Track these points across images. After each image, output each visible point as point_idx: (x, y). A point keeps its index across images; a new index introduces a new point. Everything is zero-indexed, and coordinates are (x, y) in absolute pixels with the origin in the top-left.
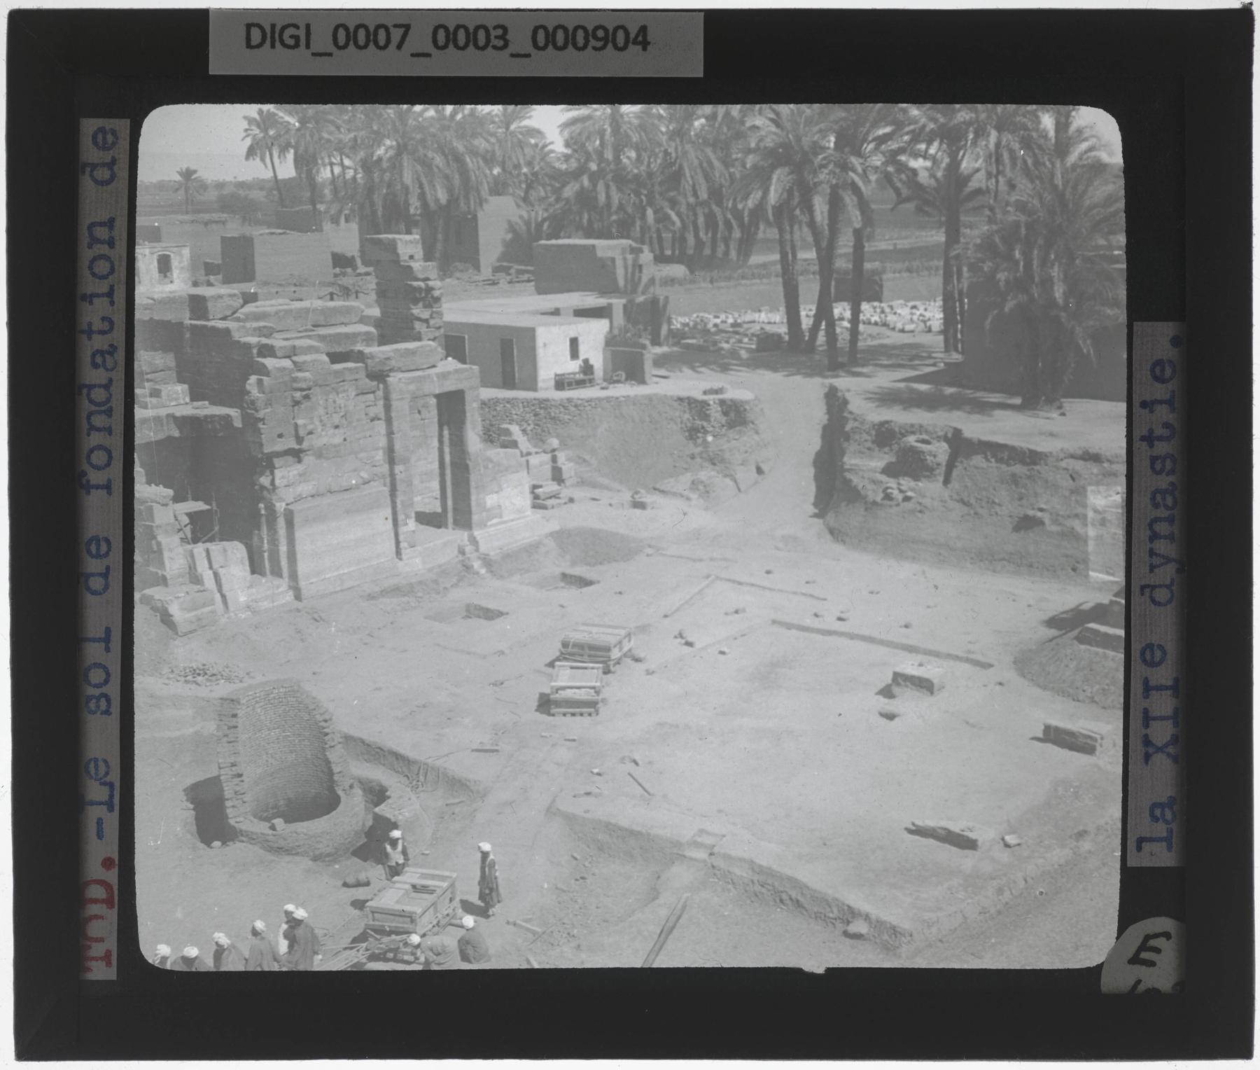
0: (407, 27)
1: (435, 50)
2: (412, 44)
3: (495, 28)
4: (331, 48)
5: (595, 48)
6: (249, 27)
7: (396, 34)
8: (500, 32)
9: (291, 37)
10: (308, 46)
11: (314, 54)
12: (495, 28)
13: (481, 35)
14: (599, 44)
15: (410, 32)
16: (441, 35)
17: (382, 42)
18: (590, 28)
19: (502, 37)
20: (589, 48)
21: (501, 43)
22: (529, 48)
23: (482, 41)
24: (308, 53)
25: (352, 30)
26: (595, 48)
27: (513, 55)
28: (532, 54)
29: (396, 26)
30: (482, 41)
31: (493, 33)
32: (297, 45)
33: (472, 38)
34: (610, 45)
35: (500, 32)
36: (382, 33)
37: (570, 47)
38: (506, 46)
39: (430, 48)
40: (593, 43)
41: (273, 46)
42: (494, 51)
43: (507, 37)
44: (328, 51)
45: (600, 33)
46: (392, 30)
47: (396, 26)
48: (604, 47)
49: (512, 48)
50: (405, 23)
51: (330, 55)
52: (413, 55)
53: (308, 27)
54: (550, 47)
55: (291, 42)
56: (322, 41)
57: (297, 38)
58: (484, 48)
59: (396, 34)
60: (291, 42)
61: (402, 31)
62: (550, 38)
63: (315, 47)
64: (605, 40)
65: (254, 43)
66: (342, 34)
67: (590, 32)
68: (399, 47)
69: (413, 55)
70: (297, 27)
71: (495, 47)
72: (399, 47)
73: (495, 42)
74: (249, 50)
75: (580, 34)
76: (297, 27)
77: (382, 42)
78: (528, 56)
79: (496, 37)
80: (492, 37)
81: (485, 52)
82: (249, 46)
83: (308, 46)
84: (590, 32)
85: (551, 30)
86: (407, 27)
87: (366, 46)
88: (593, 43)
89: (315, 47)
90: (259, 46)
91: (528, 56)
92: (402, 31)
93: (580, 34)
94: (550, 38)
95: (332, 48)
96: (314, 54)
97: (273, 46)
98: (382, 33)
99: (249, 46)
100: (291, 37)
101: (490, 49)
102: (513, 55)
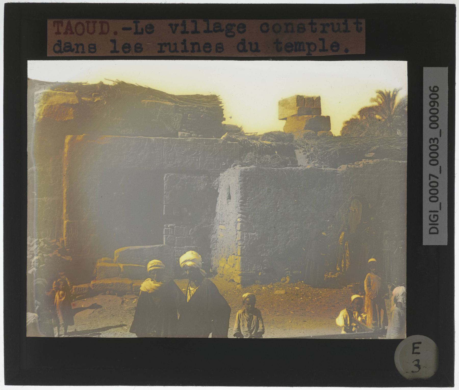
2: (437, 173)
3: (430, 143)
4: (438, 203)
5: (438, 106)
6: (430, 233)
7: (433, 179)
8: (432, 141)
9: (434, 218)
10: (437, 212)
11: (440, 209)
12: (430, 143)
13: (433, 148)
15: (432, 174)
16: (432, 162)
18: (431, 108)
20: (437, 108)
21: (436, 141)
22: (438, 130)
23: (435, 148)
26: (438, 106)
29: (430, 179)
30: (435, 148)
31: (432, 143)
32: (437, 216)
33: (434, 151)
34: (436, 100)
35: (432, 141)
36: (432, 184)
40: (436, 107)
41: (437, 224)
42: (439, 143)
43: (434, 138)
44: (439, 203)
45: (432, 104)
46: (431, 180)
47: (430, 179)
50: (429, 175)
52: (440, 173)
53: (430, 211)
55: (436, 217)
56: (435, 206)
57: (434, 216)
59: (433, 179)
61: (431, 176)
62: (434, 122)
63: (438, 209)
64: (434, 91)
65: (437, 232)
66: (432, 199)
68: (437, 178)
69: (440, 173)
70: (430, 215)
71: (437, 143)
72: (437, 178)
73: (435, 143)
74: (439, 233)
75: (433, 111)
77: (435, 184)
79: (434, 142)
80: (434, 144)
81: (439, 146)
83: (437, 212)
85: (431, 122)
87: (437, 190)
88: (436, 107)
89: (438, 209)
90: (437, 229)
93: (432, 111)
94: (434, 122)
95: (438, 202)
96: (440, 209)
97: (437, 224)
98: (432, 184)
100: (434, 218)
101: (437, 144)
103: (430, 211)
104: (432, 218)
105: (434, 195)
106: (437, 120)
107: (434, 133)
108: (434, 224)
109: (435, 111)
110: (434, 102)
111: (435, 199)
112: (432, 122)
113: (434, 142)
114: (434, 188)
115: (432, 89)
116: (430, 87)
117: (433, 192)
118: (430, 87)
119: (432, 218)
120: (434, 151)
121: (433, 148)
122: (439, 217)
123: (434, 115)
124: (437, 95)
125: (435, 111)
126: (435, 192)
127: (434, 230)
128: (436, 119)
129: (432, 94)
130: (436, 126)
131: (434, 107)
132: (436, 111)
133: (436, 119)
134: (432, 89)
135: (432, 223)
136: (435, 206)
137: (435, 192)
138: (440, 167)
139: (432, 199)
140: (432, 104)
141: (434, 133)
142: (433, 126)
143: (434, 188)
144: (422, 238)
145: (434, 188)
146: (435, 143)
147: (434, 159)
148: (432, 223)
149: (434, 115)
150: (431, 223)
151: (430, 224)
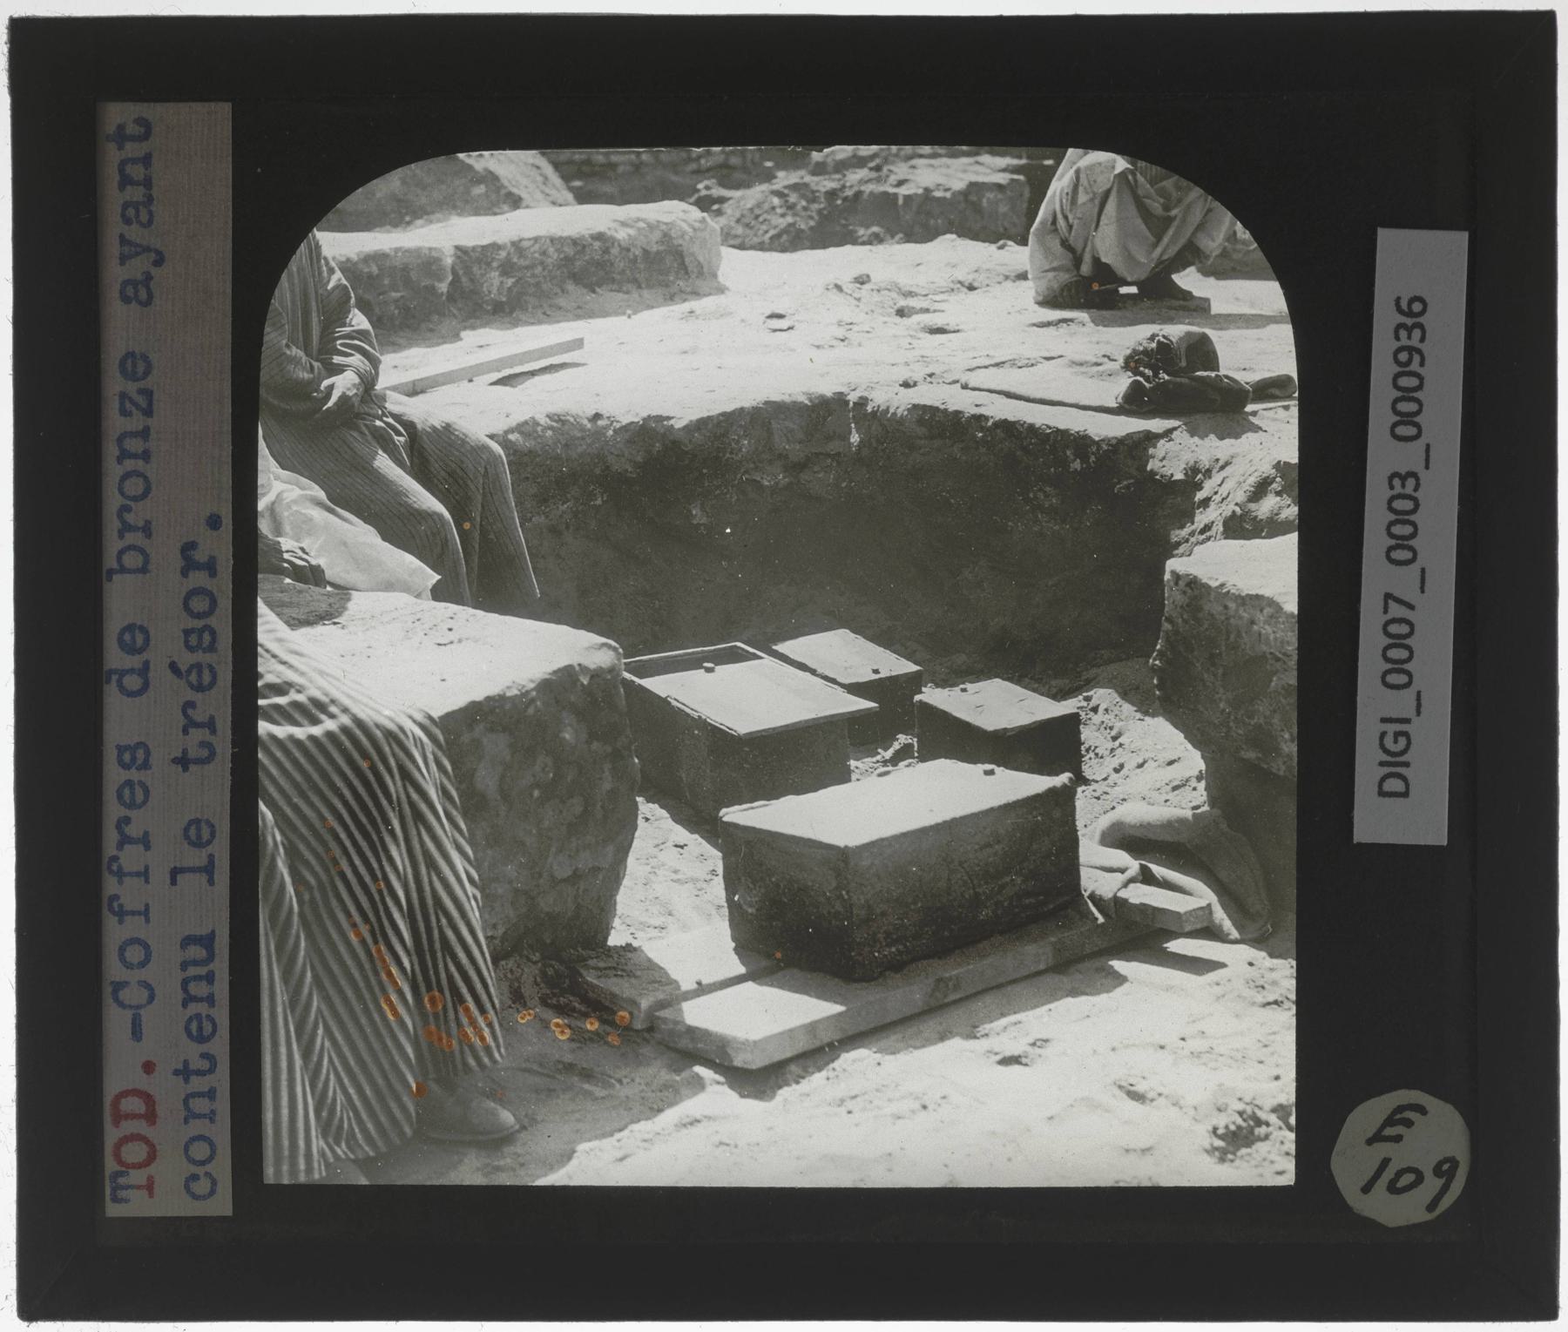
0: (1388, 596)
1: (1417, 562)
2: (1411, 595)
3: (1392, 487)
4: (1408, 696)
5: (1422, 364)
6: (1382, 793)
7: (1396, 610)
8: (1397, 482)
9: (1396, 742)
10: (1407, 721)
11: (1418, 713)
12: (1392, 487)
13: (1399, 505)
14: (1417, 358)
15: (1397, 594)
17: (1404, 629)
19: (1404, 479)
21: (1411, 482)
22: (1419, 445)
23: (1409, 505)
24: (1415, 719)
25: (1389, 666)
26: (1422, 364)
27: (1427, 467)
28: (1427, 442)
29: (1386, 612)
30: (1408, 505)
31: (1398, 490)
32: (1406, 734)
33: (1402, 517)
35: (1397, 482)
36: (1393, 629)
37: (1417, 419)
38: (1414, 475)
39: (1415, 569)
40: (1415, 366)
41: (1407, 764)
43: (1403, 472)
44: (1414, 697)
45: (1403, 357)
46: (1389, 616)
47: (1386, 612)
48: (1419, 352)
49: (1419, 467)
51: (1419, 693)
52: (1423, 592)
53: (1384, 720)
54: (1417, 419)
55: (1402, 741)
56: (1401, 703)
57: (1397, 735)
58: (1415, 500)
59: (1396, 610)
60: (1402, 741)
61: (1390, 601)
62: (1407, 419)
63: (1411, 713)
66: (1391, 679)
67: (1399, 369)
68: (1411, 607)
69: (1423, 592)
70: (1383, 735)
71: (1416, 490)
72: (1411, 607)
75: (1405, 382)
76: (1383, 735)
78: (1428, 446)
79: (1403, 486)
82: (1405, 794)
83: (1407, 721)
84: (1399, 369)
86: (1388, 596)
88: (1415, 366)
89: (1410, 712)
91: (1428, 446)
92: (1390, 601)
93: (1405, 382)
94: (1407, 419)
96: (1418, 713)
97: (1407, 764)
98: (1393, 629)
99: (1405, 794)
100: (1396, 742)
101: (1416, 495)
102: (1427, 467)
103: (1384, 720)
104: (1389, 742)
105: (1398, 667)
106: (1419, 412)
107: (1408, 457)
108: (1395, 763)
109: (1411, 382)
110: (1409, 358)
111: (1403, 679)
112: (1398, 418)
113: (1403, 486)
114: (1398, 641)
115: (1404, 305)
116: (1398, 300)
117: (1395, 654)
118: (1398, 300)
119: (1389, 742)
120: (1402, 517)
121: (1399, 505)
122: (1412, 737)
123: (1407, 394)
124: (1414, 524)
125: (1414, 382)
126: (1404, 654)
127: (1394, 785)
128: (1413, 407)
129: (1397, 522)
130: (1412, 431)
131: (1407, 369)
132: (1414, 382)
133: (1413, 407)
134: (1404, 305)
135: (1389, 759)
136: (1401, 703)
137: (1404, 654)
138: (1423, 571)
139: (1391, 679)
140: (1403, 357)
141: (1408, 457)
142: (1402, 430)
143: (1400, 639)
144: (1359, 575)
145: (1398, 641)
146: (1409, 490)
147: (1402, 543)
148: (1389, 759)
149: (1407, 394)
150: (1384, 760)
151: (1382, 764)
